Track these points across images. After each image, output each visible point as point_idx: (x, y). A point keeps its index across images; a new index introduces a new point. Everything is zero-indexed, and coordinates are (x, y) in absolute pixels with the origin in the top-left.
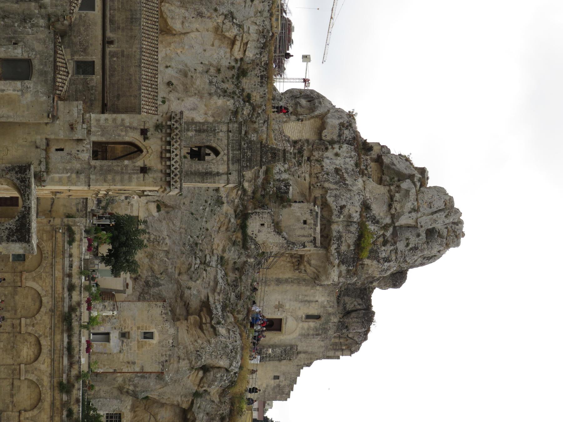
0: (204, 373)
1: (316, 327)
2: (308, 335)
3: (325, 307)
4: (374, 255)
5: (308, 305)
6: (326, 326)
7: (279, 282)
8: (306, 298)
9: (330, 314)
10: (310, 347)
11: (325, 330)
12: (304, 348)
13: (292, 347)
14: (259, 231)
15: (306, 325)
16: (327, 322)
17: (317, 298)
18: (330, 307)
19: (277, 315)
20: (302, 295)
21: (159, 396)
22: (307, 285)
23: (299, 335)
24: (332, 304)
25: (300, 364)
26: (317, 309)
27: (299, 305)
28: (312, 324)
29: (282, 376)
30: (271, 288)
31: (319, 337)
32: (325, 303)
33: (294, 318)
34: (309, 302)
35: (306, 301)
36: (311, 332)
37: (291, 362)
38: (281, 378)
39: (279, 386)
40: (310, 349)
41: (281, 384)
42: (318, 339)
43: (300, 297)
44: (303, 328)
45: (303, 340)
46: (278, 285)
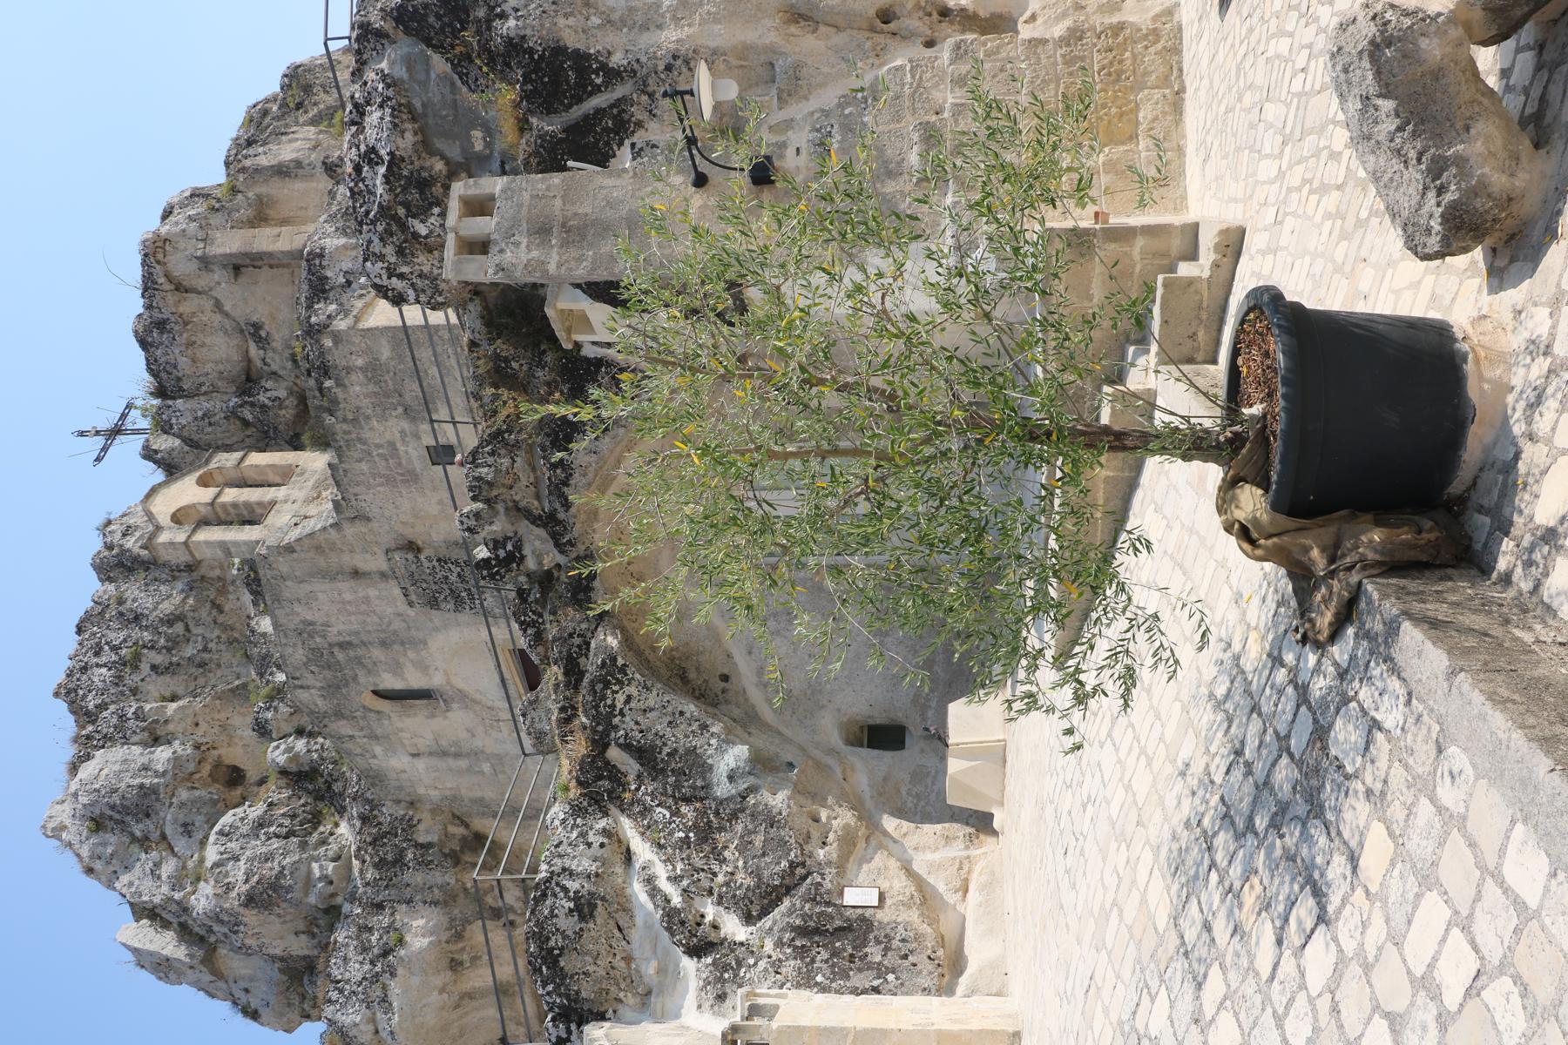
2: (384, 644)
3: (375, 737)
5: (444, 743)
6: (328, 674)
8: (463, 763)
9: (339, 715)
10: (348, 596)
12: (372, 592)
13: (433, 603)
15: (414, 680)
17: (421, 764)
18: (351, 737)
20: (482, 773)
22: (480, 801)
23: (426, 643)
24: (349, 745)
25: (360, 527)
26: (401, 730)
27: (478, 743)
28: (390, 682)
29: (418, 466)
31: (333, 639)
32: (378, 750)
33: (474, 701)
34: (444, 754)
35: (457, 755)
37: (409, 533)
38: (414, 454)
40: (347, 590)
41: (405, 425)
42: (334, 630)
43: (486, 767)
45: (397, 625)
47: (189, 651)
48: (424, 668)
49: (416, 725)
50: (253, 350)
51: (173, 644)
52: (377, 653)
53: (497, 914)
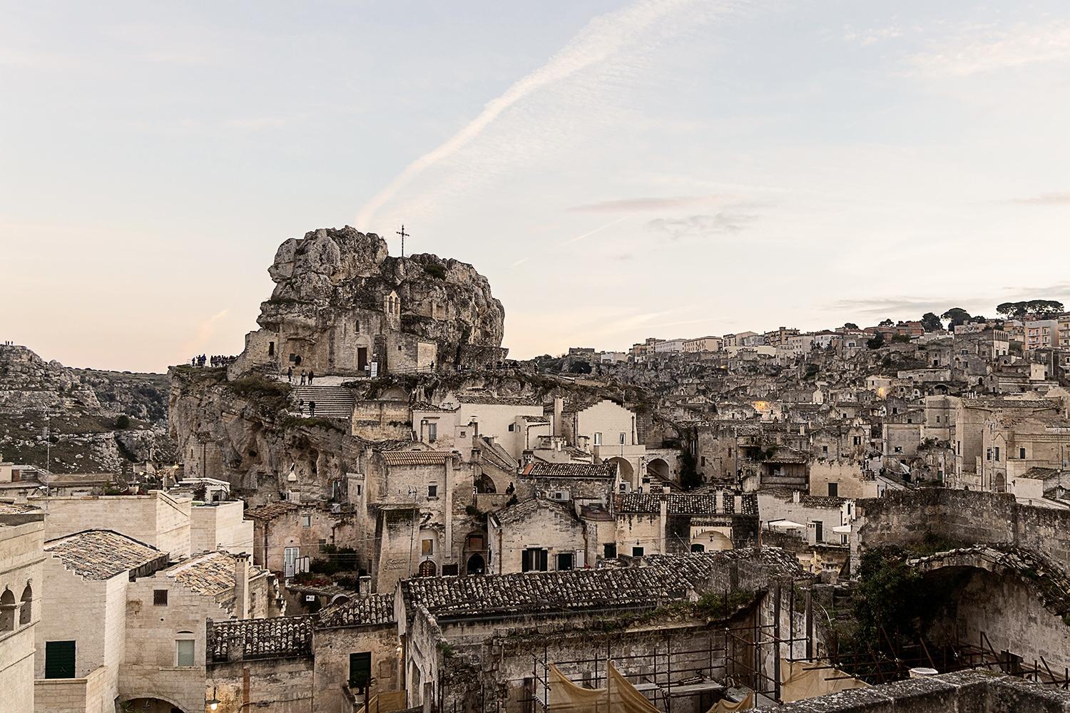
0: (224, 411)
1: (363, 323)
2: (368, 328)
3: (349, 318)
4: (298, 290)
7: (332, 353)
11: (365, 316)
14: (234, 373)
15: (361, 330)
16: (359, 315)
17: (343, 325)
19: (356, 351)
21: (241, 445)
28: (361, 326)
30: (336, 358)
36: (367, 326)
38: (400, 344)
39: (406, 346)
44: (363, 333)
46: (334, 353)
47: (358, 264)
48: (363, 333)
49: (351, 327)
50: (418, 302)
51: (359, 261)
52: (367, 326)
53: (312, 334)
